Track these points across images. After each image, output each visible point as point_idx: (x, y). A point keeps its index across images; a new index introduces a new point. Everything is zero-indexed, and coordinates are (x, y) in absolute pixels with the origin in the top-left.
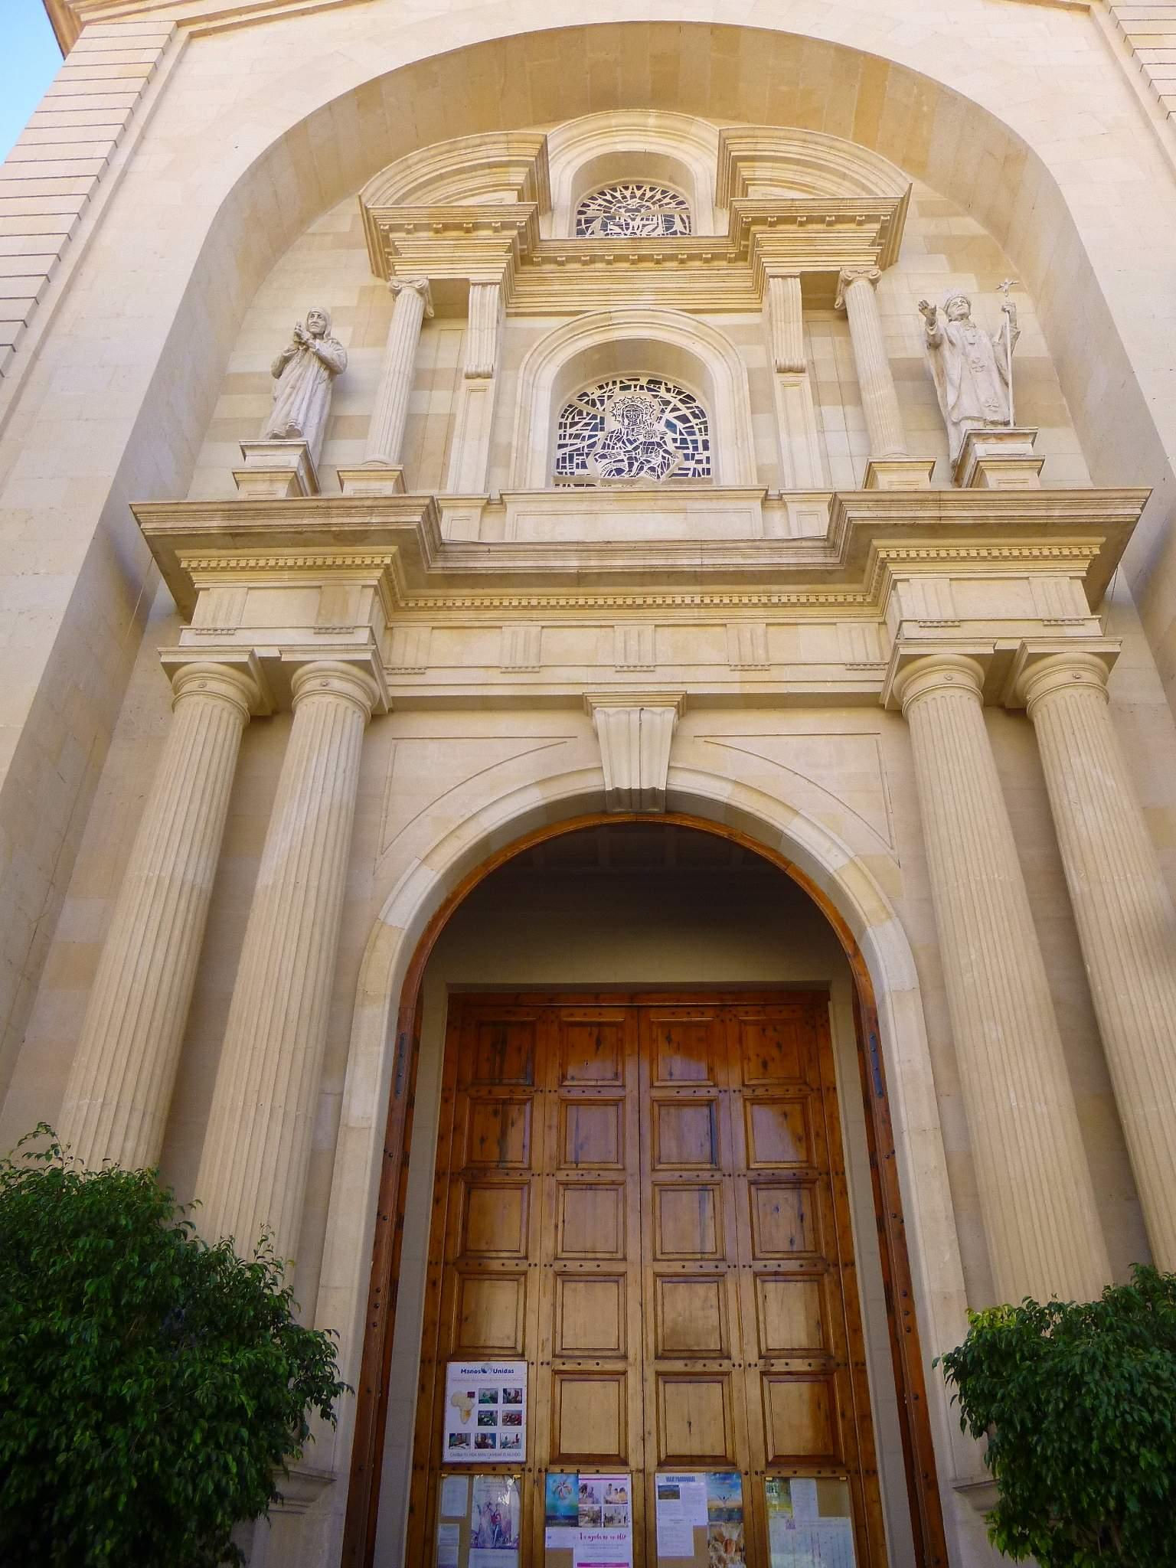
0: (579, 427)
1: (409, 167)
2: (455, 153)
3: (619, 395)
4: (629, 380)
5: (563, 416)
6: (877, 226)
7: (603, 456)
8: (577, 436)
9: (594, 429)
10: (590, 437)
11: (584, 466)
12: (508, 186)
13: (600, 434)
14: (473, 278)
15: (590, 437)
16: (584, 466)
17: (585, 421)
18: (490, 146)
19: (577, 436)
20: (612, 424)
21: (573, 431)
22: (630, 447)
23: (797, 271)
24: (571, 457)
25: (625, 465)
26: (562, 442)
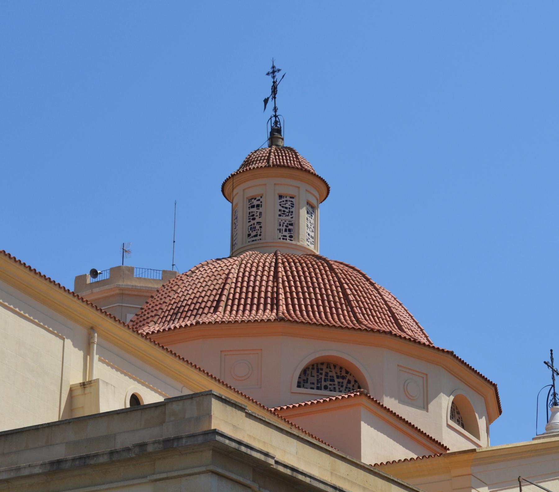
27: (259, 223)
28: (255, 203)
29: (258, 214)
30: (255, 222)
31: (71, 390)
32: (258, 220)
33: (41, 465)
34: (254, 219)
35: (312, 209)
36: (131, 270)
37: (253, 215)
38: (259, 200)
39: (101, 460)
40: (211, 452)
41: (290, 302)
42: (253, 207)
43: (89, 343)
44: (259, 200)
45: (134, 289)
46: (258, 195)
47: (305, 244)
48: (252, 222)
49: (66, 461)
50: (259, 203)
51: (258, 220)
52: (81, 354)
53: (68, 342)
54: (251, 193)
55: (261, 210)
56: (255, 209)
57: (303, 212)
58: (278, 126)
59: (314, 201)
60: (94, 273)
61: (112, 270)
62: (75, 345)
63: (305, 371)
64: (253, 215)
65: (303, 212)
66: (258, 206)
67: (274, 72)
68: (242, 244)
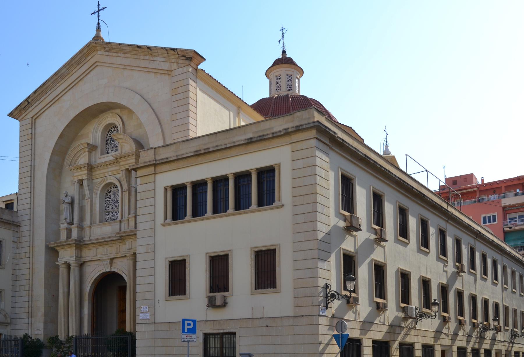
0: (108, 198)
1: (70, 155)
2: (76, 149)
3: (113, 190)
4: (114, 185)
5: (106, 196)
6: (134, 156)
7: (111, 205)
8: (107, 201)
9: (110, 199)
10: (109, 200)
11: (108, 208)
12: (86, 151)
13: (110, 199)
14: (84, 178)
15: (109, 200)
16: (108, 208)
17: (108, 197)
18: (80, 146)
19: (107, 201)
20: (112, 197)
21: (107, 199)
22: (114, 202)
23: (124, 169)
24: (107, 205)
25: (113, 207)
26: (106, 202)
27: (280, 85)
28: (278, 78)
29: (279, 82)
30: (279, 84)
32: (279, 84)
33: (244, 140)
34: (278, 84)
37: (277, 82)
38: (279, 77)
39: (269, 136)
40: (315, 130)
42: (277, 79)
44: (279, 77)
46: (279, 75)
48: (277, 85)
49: (254, 138)
50: (279, 78)
51: (279, 84)
54: (276, 74)
55: (280, 80)
56: (278, 80)
58: (285, 50)
64: (277, 82)
66: (279, 79)
68: (274, 92)
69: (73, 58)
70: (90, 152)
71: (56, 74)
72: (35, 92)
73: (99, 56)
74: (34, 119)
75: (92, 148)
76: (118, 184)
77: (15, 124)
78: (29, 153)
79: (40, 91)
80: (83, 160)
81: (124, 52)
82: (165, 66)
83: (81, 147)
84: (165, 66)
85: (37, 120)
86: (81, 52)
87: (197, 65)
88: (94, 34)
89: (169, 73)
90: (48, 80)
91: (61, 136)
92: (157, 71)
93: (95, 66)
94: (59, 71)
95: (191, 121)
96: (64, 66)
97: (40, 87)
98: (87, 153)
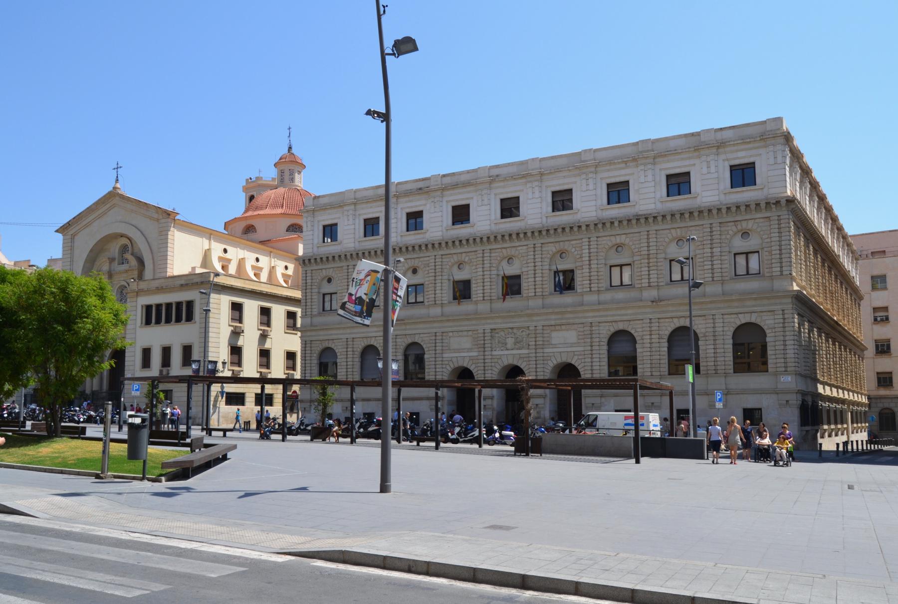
31: (205, 250)
35: (299, 173)
36: (262, 178)
41: (287, 207)
43: (210, 238)
45: (262, 184)
47: (297, 184)
52: (208, 241)
53: (204, 239)
57: (296, 174)
59: (300, 170)
60: (251, 179)
61: (256, 178)
62: (206, 239)
63: (289, 227)
65: (296, 174)
67: (289, 128)
69: (99, 200)
70: (110, 263)
71: (88, 208)
72: (74, 218)
73: (116, 200)
74: (73, 237)
75: (112, 260)
76: (127, 286)
77: (60, 236)
78: (69, 260)
79: (77, 218)
80: (106, 268)
81: (132, 202)
82: (156, 216)
83: (104, 260)
84: (156, 216)
85: (75, 237)
86: (105, 196)
87: (175, 217)
88: (112, 184)
89: (158, 220)
90: (83, 212)
91: (91, 251)
92: (151, 218)
93: (113, 206)
94: (90, 207)
95: (169, 253)
96: (94, 204)
97: (78, 215)
98: (108, 264)
